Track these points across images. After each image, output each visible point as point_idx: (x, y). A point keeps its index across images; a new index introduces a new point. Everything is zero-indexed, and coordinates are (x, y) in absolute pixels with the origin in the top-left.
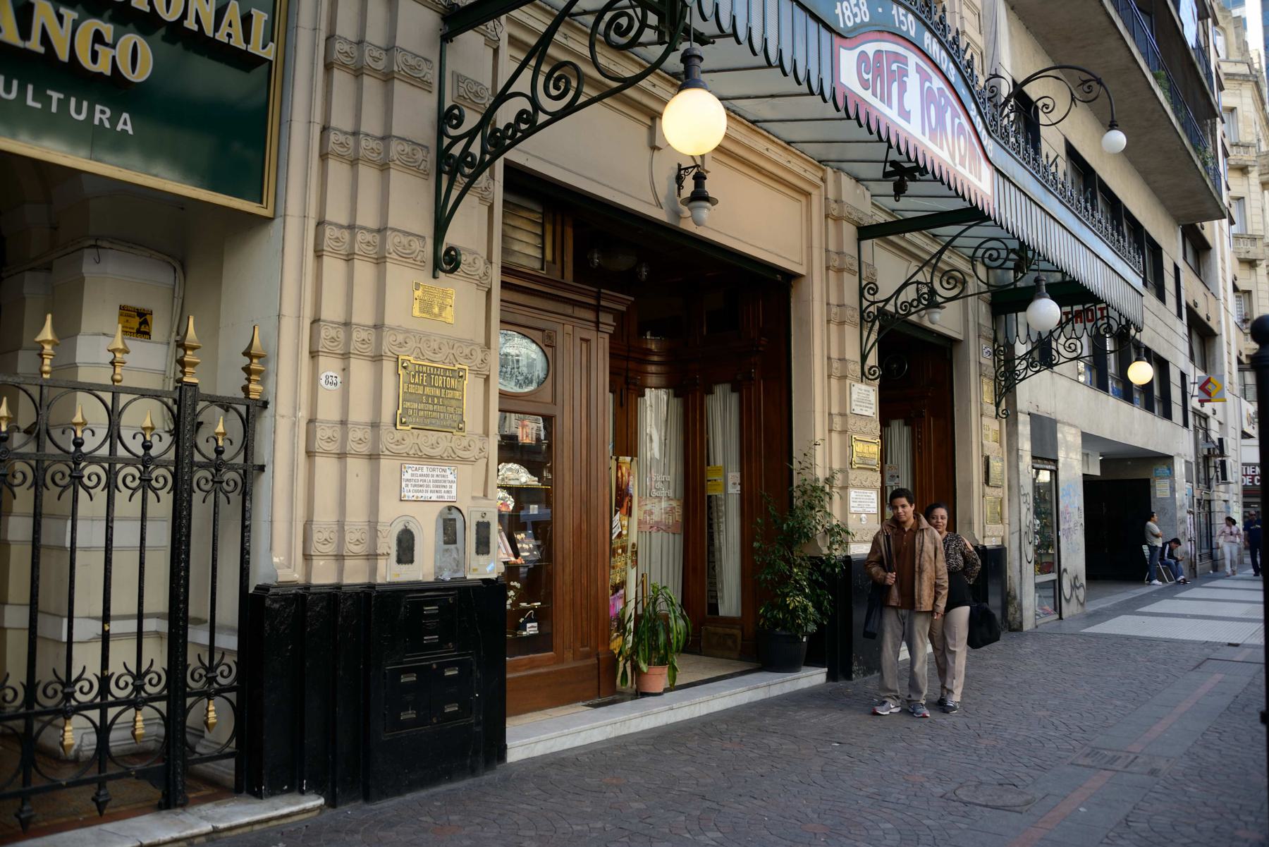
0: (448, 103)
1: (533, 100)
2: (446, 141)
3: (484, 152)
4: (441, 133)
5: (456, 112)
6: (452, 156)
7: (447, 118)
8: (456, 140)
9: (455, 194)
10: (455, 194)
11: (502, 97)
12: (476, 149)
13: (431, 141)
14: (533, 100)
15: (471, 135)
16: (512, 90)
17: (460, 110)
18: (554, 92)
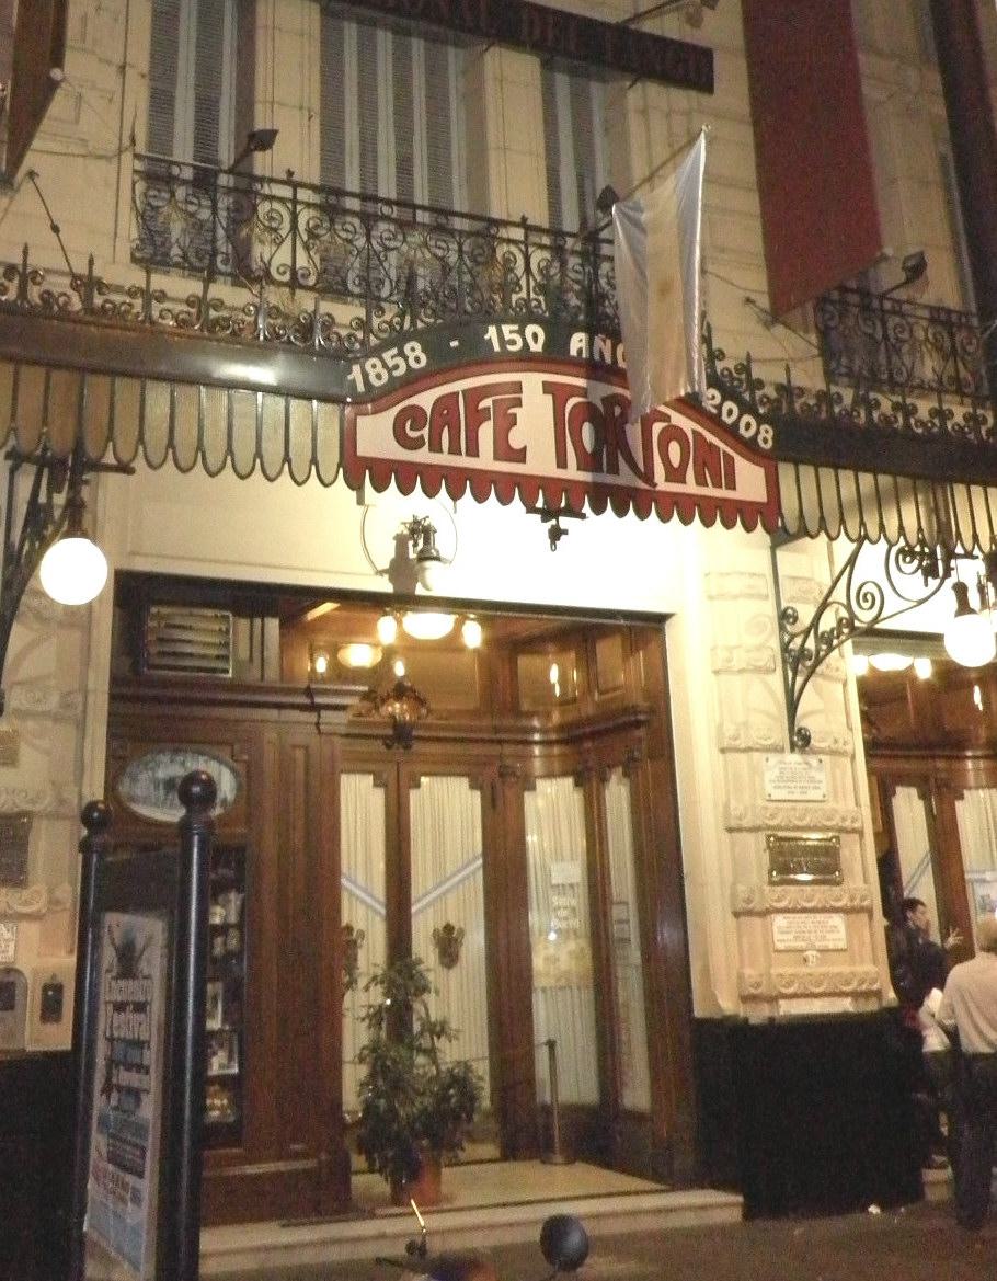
0: (784, 605)
1: (849, 607)
2: (786, 638)
3: (818, 651)
4: (782, 628)
5: (790, 611)
6: (791, 650)
7: (786, 617)
8: (793, 637)
9: (799, 680)
10: (799, 680)
11: (824, 605)
12: (811, 644)
13: (775, 644)
14: (849, 607)
15: (807, 633)
16: (830, 600)
17: (794, 611)
18: (866, 605)
